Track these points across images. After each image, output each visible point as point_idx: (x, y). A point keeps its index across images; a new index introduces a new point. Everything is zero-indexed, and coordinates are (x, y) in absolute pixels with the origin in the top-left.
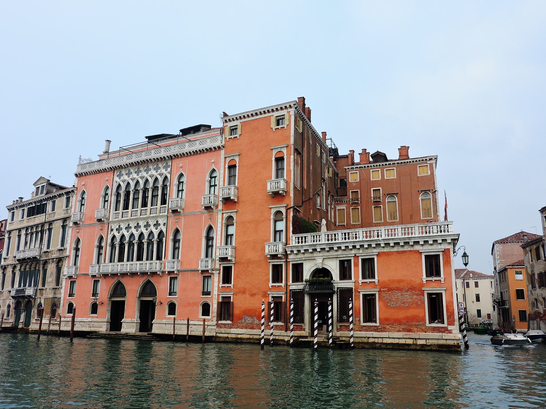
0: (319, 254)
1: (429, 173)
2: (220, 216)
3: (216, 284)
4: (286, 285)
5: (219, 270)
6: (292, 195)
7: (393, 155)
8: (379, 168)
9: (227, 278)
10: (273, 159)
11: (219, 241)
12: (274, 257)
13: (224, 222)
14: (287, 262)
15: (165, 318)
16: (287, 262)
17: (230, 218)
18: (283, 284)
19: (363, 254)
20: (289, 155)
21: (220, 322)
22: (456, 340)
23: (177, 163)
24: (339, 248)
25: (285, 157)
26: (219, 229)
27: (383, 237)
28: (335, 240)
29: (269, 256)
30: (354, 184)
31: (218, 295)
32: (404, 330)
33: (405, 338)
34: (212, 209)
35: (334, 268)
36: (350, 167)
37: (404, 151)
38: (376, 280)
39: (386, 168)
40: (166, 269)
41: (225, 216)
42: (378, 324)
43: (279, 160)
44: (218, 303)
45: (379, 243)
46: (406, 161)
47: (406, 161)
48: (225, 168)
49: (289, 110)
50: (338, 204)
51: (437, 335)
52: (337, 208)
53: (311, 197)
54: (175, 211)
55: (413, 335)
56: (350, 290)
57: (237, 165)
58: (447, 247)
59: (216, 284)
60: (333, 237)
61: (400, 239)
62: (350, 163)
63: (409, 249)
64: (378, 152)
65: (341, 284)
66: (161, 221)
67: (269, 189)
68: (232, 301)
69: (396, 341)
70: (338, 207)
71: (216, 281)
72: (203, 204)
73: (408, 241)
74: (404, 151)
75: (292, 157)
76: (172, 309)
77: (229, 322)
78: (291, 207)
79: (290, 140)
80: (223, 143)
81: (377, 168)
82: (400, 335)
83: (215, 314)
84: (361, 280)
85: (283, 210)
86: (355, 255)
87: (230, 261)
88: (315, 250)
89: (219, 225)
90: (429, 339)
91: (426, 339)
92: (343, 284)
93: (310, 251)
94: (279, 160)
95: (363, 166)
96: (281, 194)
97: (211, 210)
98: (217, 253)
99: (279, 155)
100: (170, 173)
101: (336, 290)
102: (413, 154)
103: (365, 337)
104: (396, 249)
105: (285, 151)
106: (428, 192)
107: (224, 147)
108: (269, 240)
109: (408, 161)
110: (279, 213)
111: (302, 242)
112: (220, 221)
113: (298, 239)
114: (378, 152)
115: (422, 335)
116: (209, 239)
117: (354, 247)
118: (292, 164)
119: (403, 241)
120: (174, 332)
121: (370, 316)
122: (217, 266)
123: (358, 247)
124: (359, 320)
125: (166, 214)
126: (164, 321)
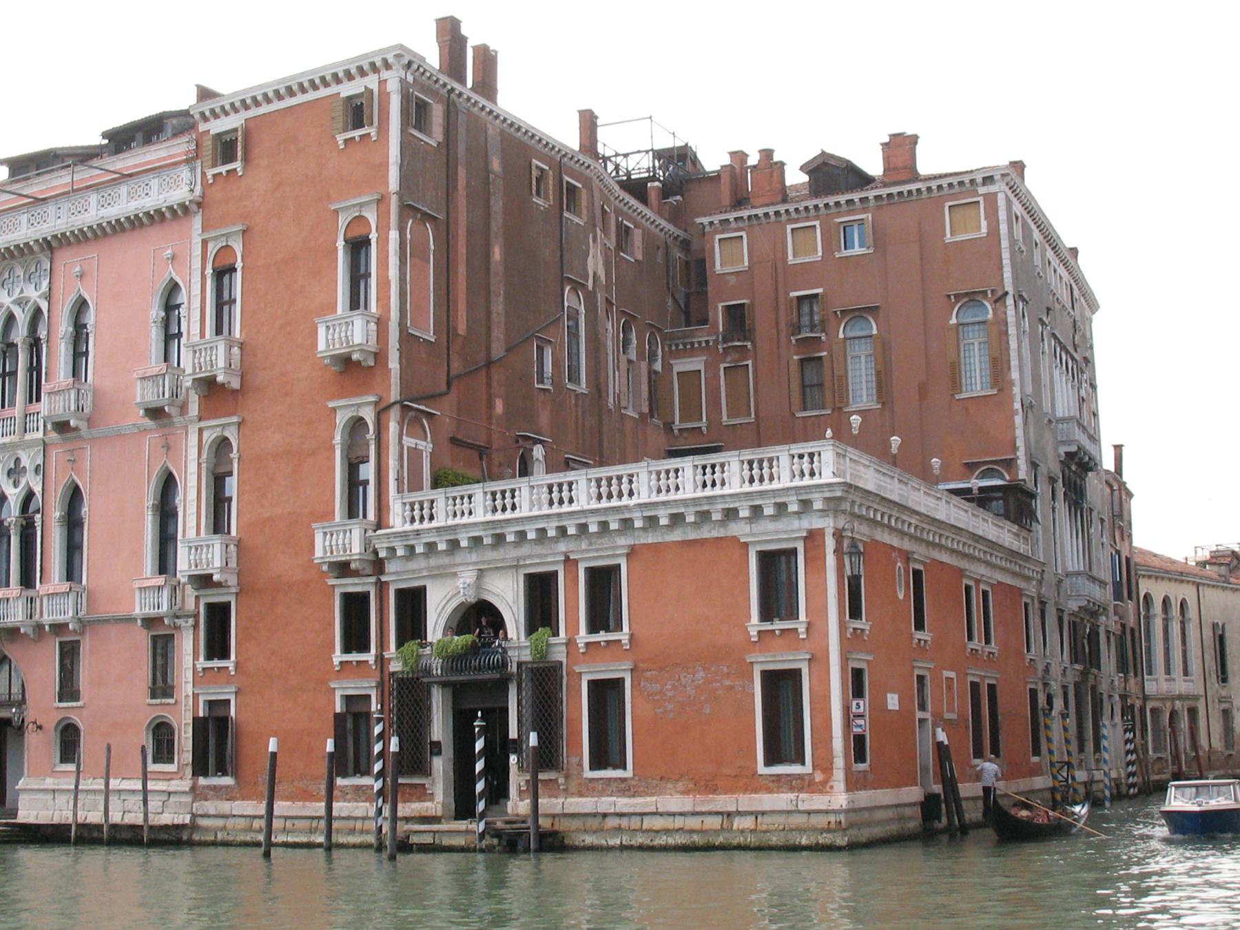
1: (984, 230)
2: (193, 440)
3: (188, 661)
4: (381, 661)
5: (196, 616)
6: (394, 364)
7: (873, 165)
8: (817, 218)
9: (217, 646)
10: (340, 243)
11: (192, 522)
12: (343, 569)
13: (204, 456)
14: (382, 587)
15: (53, 773)
16: (382, 587)
17: (223, 444)
18: (370, 657)
19: (592, 555)
20: (383, 229)
21: (202, 781)
22: (834, 812)
23: (70, 262)
24: (522, 535)
25: (373, 236)
26: (192, 481)
27: (644, 499)
29: (325, 568)
30: (732, 280)
31: (196, 696)
34: (169, 416)
35: (509, 597)
36: (716, 219)
37: (900, 149)
38: (624, 636)
39: (839, 214)
40: (45, 616)
41: (209, 437)
42: (628, 773)
43: (358, 246)
44: (196, 720)
45: (627, 516)
46: (905, 188)
47: (905, 188)
48: (203, 277)
49: (385, 74)
50: (677, 354)
51: (782, 800)
52: (676, 369)
53: (498, 351)
54: (62, 427)
55: (724, 802)
57: (239, 265)
58: (817, 523)
59: (188, 661)
60: (508, 501)
61: (684, 502)
62: (726, 199)
63: (715, 534)
64: (823, 153)
66: (28, 460)
67: (321, 346)
68: (233, 713)
69: (679, 822)
70: (681, 366)
71: (188, 652)
72: (138, 400)
73: (706, 508)
74: (900, 149)
75: (394, 235)
76: (69, 741)
77: (228, 781)
78: (395, 403)
79: (386, 176)
80: (198, 189)
81: (807, 219)
83: (188, 757)
85: (369, 415)
87: (219, 585)
88: (454, 545)
89: (193, 468)
90: (763, 813)
91: (756, 814)
93: (442, 547)
94: (358, 246)
95: (760, 212)
96: (359, 362)
97: (166, 421)
98: (184, 563)
99: (357, 232)
100: (49, 297)
101: (515, 669)
102: (927, 164)
103: (595, 815)
104: (677, 535)
105: (371, 216)
106: (979, 298)
107: (199, 205)
108: (329, 515)
109: (913, 187)
110: (357, 424)
111: (422, 518)
112: (193, 453)
114: (823, 153)
115: (747, 801)
116: (166, 513)
117: (562, 531)
118: (393, 261)
119: (692, 509)
120: (75, 814)
121: (606, 752)
122: (190, 605)
123: (571, 531)
124: (580, 765)
125: (40, 435)
126: (49, 783)
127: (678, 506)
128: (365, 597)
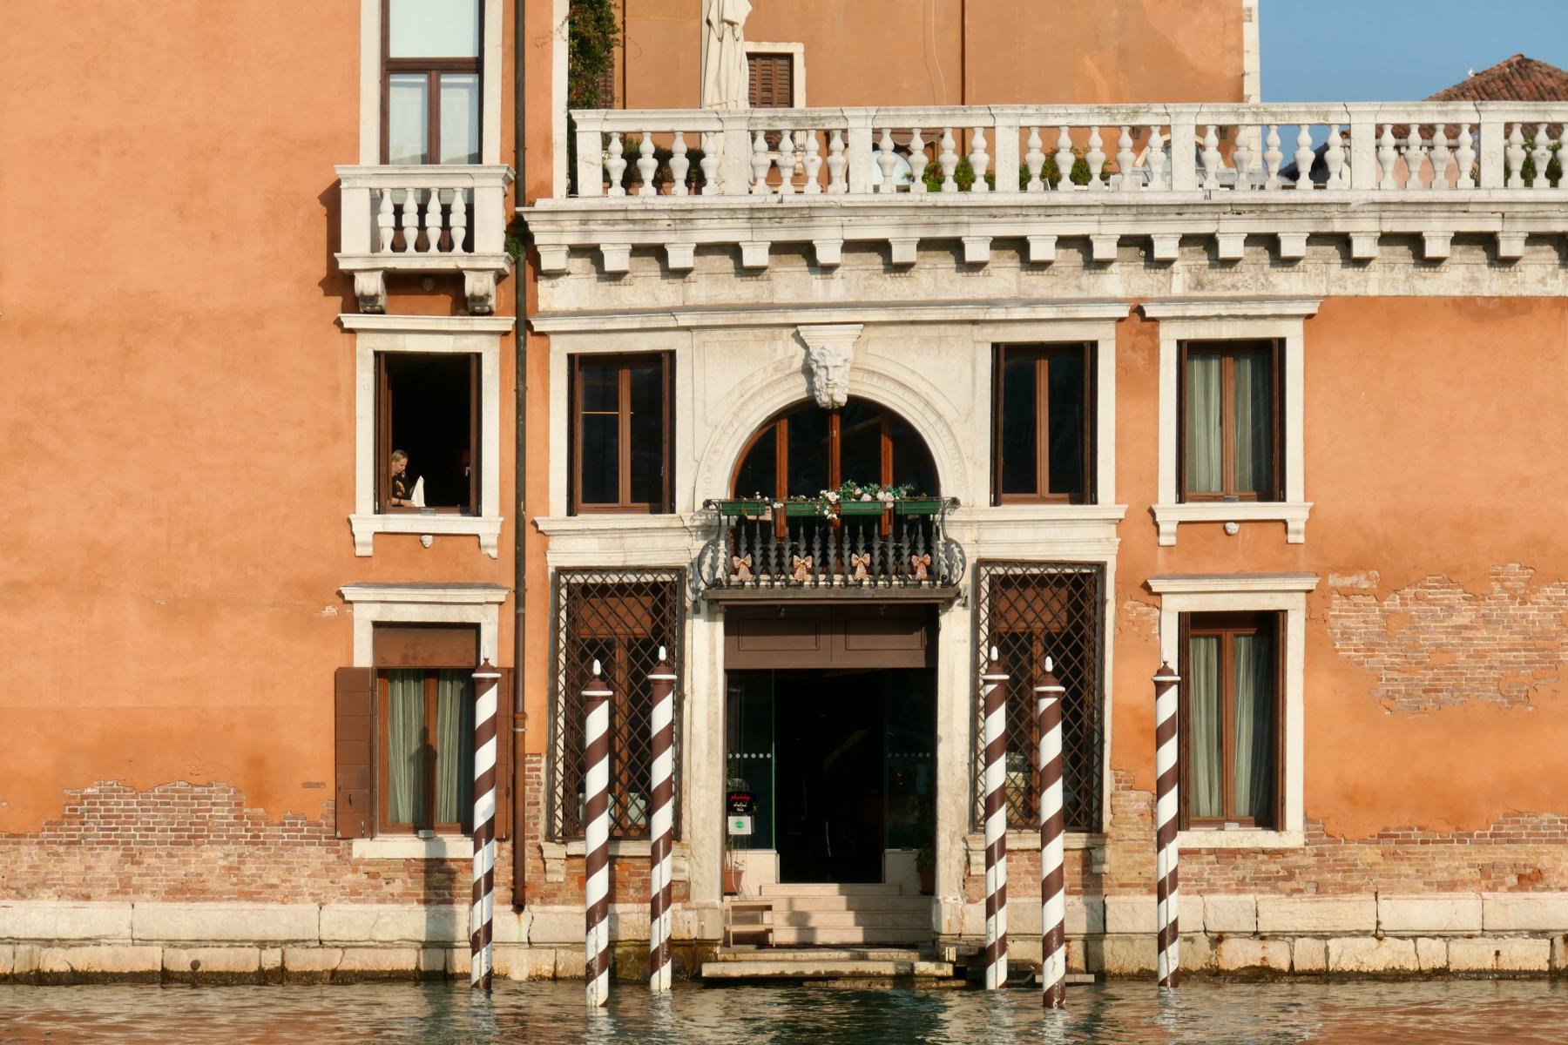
0: (817, 288)
28: (965, 179)
32: (1489, 877)
33: (1498, 934)
38: (1294, 509)
56: (1079, 587)
65: (1004, 534)
82: (1463, 909)
84: (1170, 512)
86: (1139, 311)
92: (1025, 534)
113: (632, 155)
127: (1481, 216)
128: (463, 369)
